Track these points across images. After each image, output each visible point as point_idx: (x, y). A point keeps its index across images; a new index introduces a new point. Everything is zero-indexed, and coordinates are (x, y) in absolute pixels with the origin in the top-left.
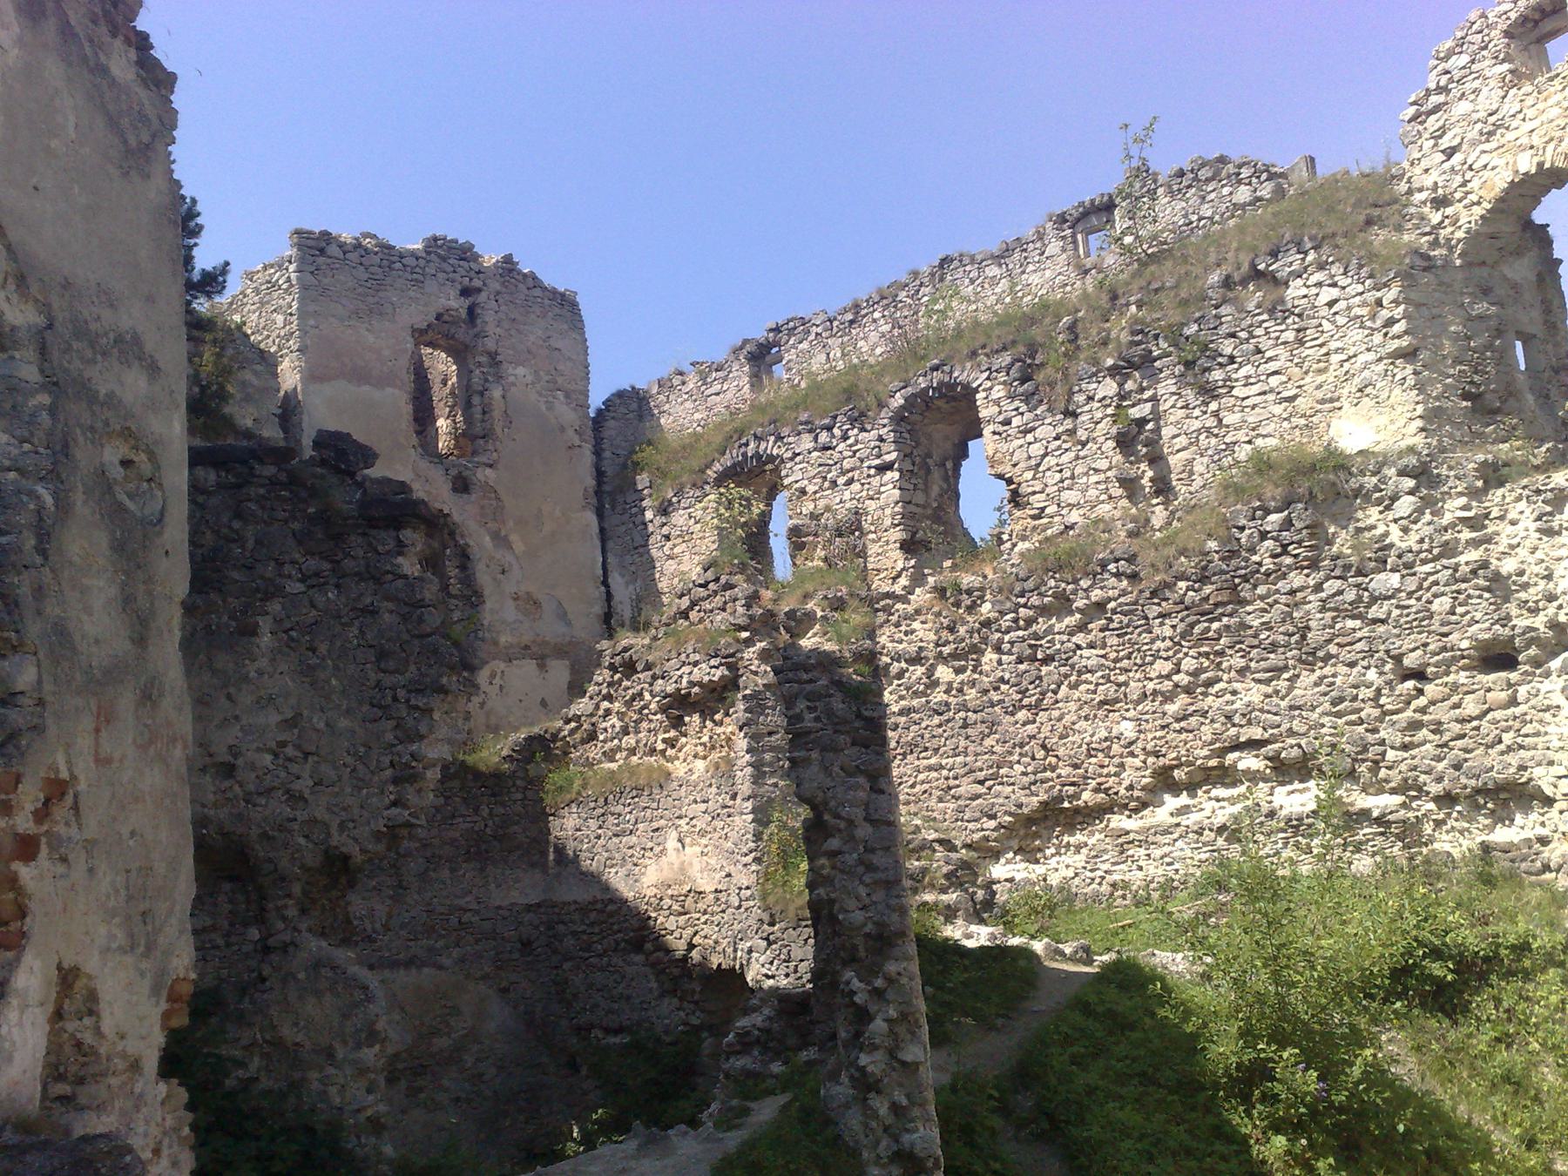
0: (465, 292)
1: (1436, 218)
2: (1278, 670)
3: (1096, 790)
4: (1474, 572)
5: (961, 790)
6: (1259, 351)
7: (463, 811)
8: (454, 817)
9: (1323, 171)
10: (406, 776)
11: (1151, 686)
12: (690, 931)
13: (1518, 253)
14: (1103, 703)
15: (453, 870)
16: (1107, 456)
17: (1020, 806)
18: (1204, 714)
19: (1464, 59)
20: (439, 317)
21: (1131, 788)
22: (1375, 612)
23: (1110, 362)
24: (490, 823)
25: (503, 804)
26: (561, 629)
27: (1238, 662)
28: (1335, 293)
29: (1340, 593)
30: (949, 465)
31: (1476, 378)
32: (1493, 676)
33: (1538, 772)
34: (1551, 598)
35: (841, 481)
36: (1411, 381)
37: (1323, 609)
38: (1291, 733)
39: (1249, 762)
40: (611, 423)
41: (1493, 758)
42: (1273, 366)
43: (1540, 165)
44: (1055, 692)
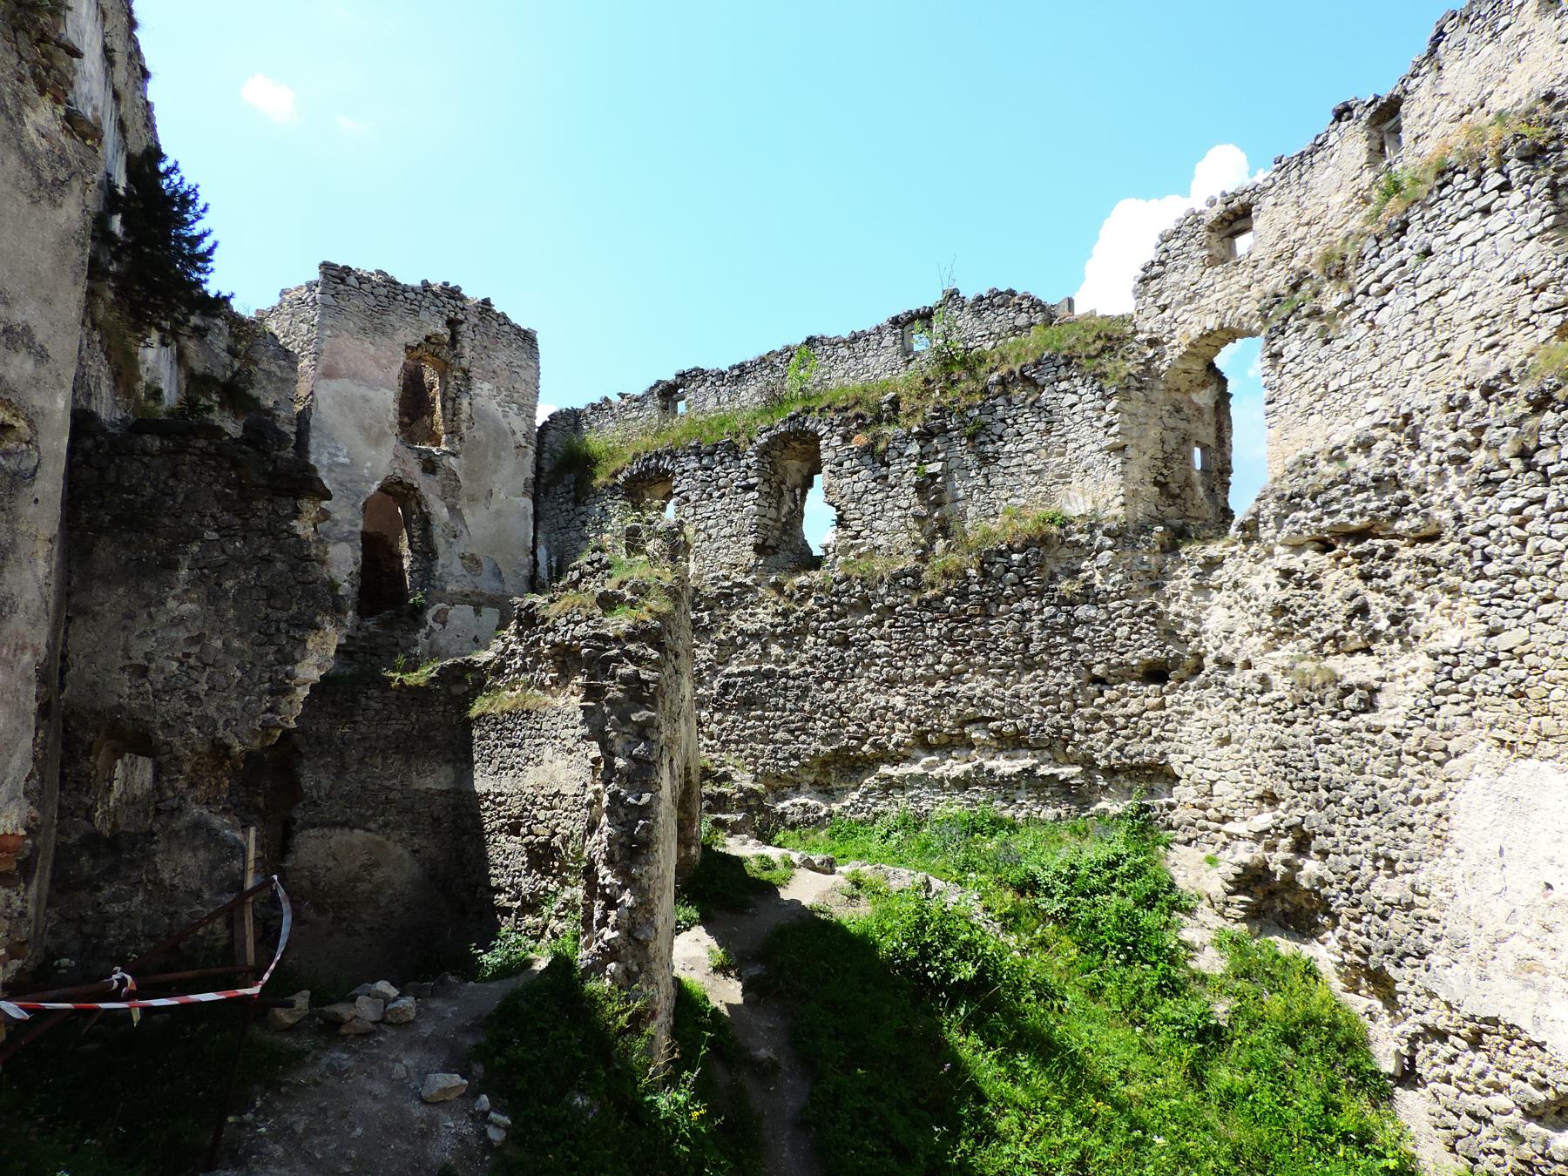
0: (452, 323)
1: (1150, 353)
2: (1007, 668)
3: (874, 744)
4: (1146, 610)
5: (777, 736)
6: (1019, 434)
7: (397, 715)
9: (1079, 310)
10: (282, 689)
11: (919, 671)
12: (554, 822)
13: (1203, 385)
14: (885, 681)
15: (384, 759)
16: (908, 498)
17: (817, 751)
18: (953, 695)
19: (1180, 242)
20: (428, 339)
21: (897, 745)
22: (1078, 632)
23: (916, 429)
26: (495, 584)
27: (980, 659)
28: (1075, 398)
29: (1054, 616)
30: (798, 491)
31: (1165, 472)
32: (1151, 686)
33: (1171, 757)
34: (1196, 634)
35: (716, 494)
36: (1119, 469)
37: (1043, 625)
38: (1013, 716)
39: (977, 735)
40: (553, 432)
41: (1145, 746)
42: (1027, 446)
43: (1221, 325)
44: (852, 670)
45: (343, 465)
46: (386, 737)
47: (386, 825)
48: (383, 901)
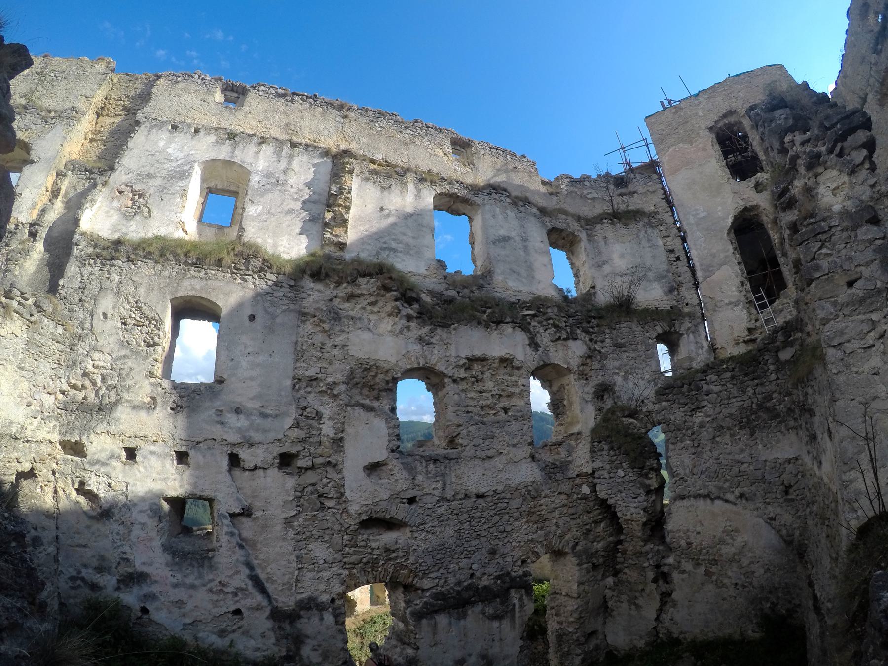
8: (729, 398)
15: (732, 435)
24: (755, 400)
25: (762, 384)
46: (730, 416)
47: (742, 496)
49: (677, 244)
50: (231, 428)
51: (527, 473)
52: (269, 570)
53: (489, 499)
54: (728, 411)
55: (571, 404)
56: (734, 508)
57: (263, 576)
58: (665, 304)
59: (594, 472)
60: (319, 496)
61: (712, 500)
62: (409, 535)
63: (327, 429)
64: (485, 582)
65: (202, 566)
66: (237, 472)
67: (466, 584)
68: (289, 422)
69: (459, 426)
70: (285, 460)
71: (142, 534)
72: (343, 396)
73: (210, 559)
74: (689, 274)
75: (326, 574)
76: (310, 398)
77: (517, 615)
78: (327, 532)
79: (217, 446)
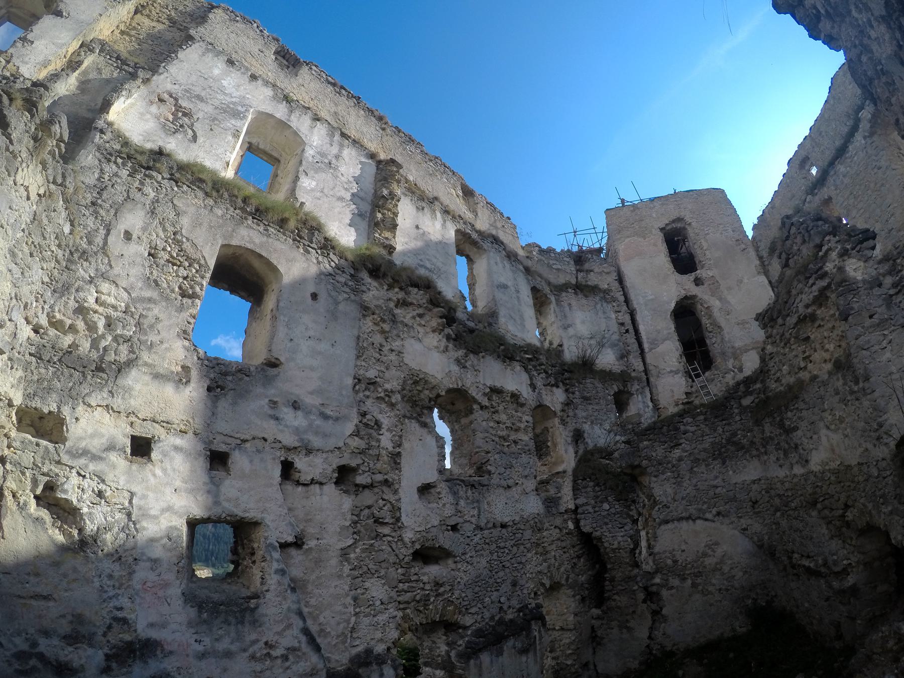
8: (703, 436)
15: (707, 465)
24: (724, 437)
25: (729, 424)
45: (652, 300)
46: (705, 450)
47: (719, 514)
48: (726, 569)
49: (627, 319)
50: (286, 426)
51: (533, 506)
52: (321, 619)
53: (510, 529)
54: (703, 446)
55: (555, 445)
56: (713, 525)
57: (314, 629)
58: (617, 368)
59: (577, 507)
60: (375, 522)
61: (694, 520)
62: (453, 566)
63: (386, 441)
64: (510, 616)
65: (242, 623)
66: (289, 487)
67: (497, 618)
68: (350, 428)
69: (488, 452)
70: (344, 475)
71: (152, 577)
72: (399, 406)
73: (253, 610)
74: (636, 346)
75: (382, 618)
76: (369, 402)
77: (538, 648)
78: (384, 565)
79: (267, 448)
